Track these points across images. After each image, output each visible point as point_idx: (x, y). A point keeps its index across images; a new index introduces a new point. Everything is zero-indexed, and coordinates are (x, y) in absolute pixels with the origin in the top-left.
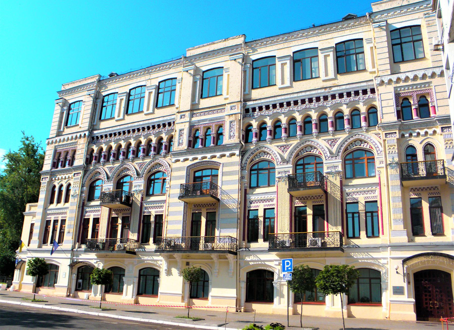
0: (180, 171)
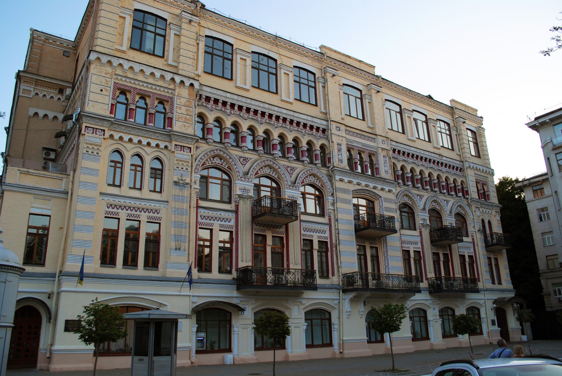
0: (345, 193)
